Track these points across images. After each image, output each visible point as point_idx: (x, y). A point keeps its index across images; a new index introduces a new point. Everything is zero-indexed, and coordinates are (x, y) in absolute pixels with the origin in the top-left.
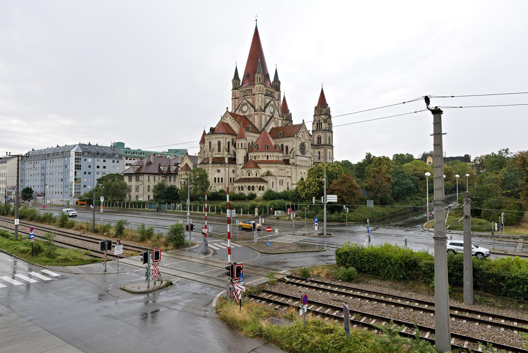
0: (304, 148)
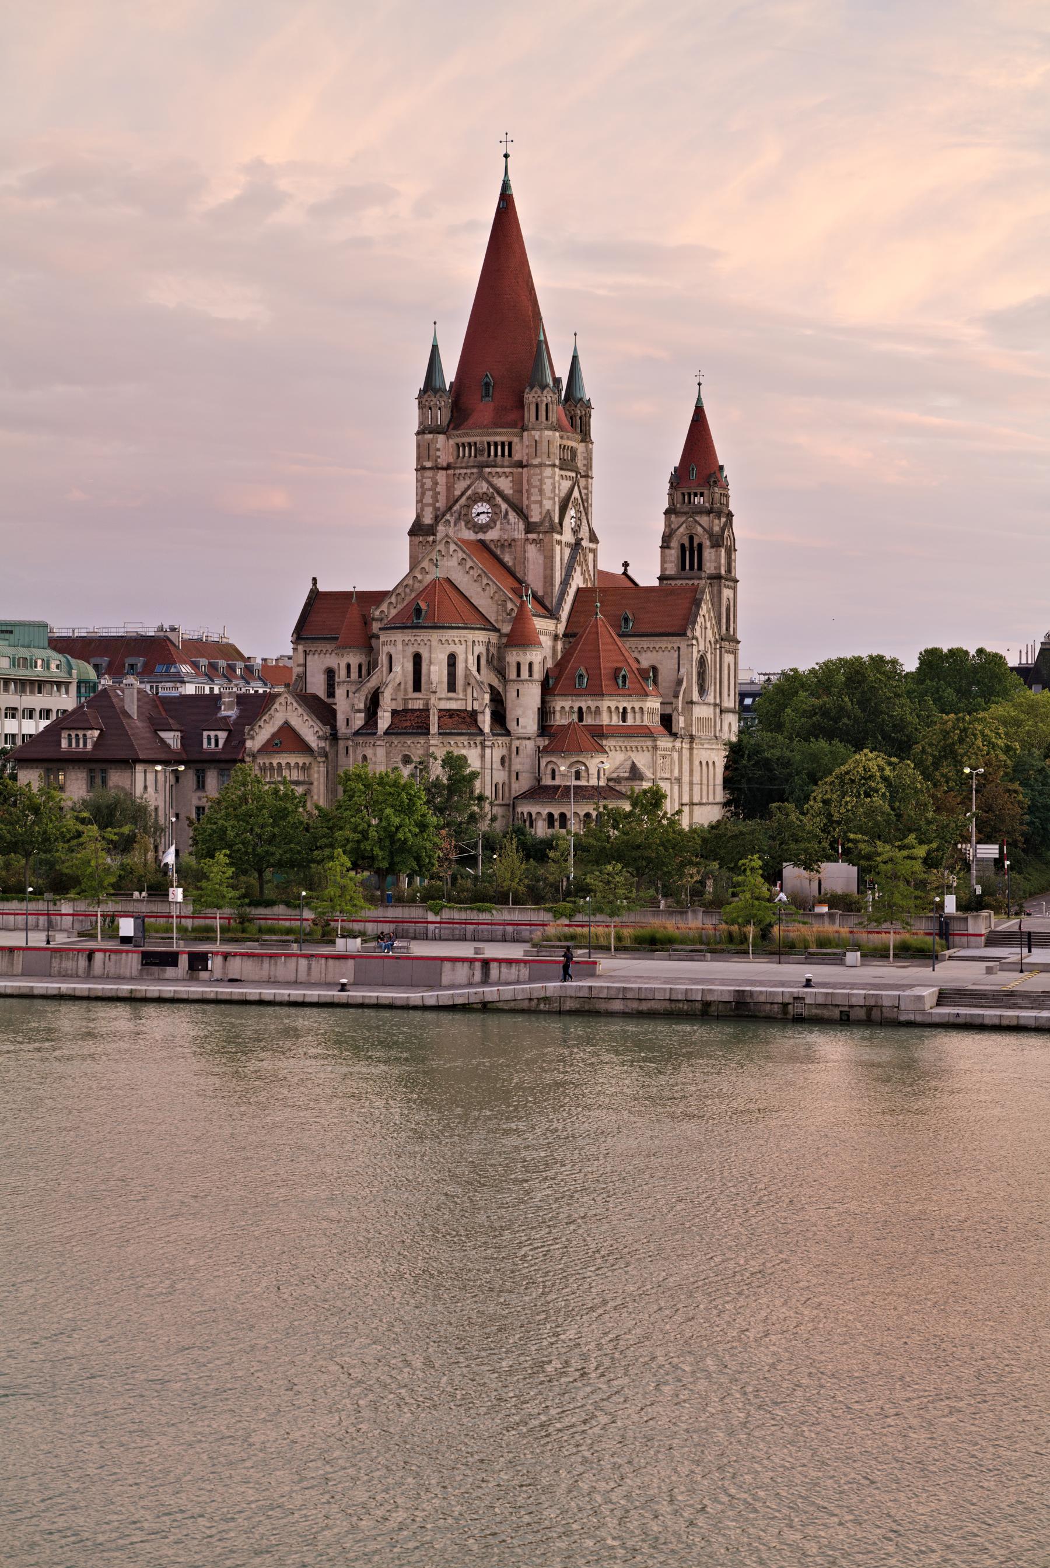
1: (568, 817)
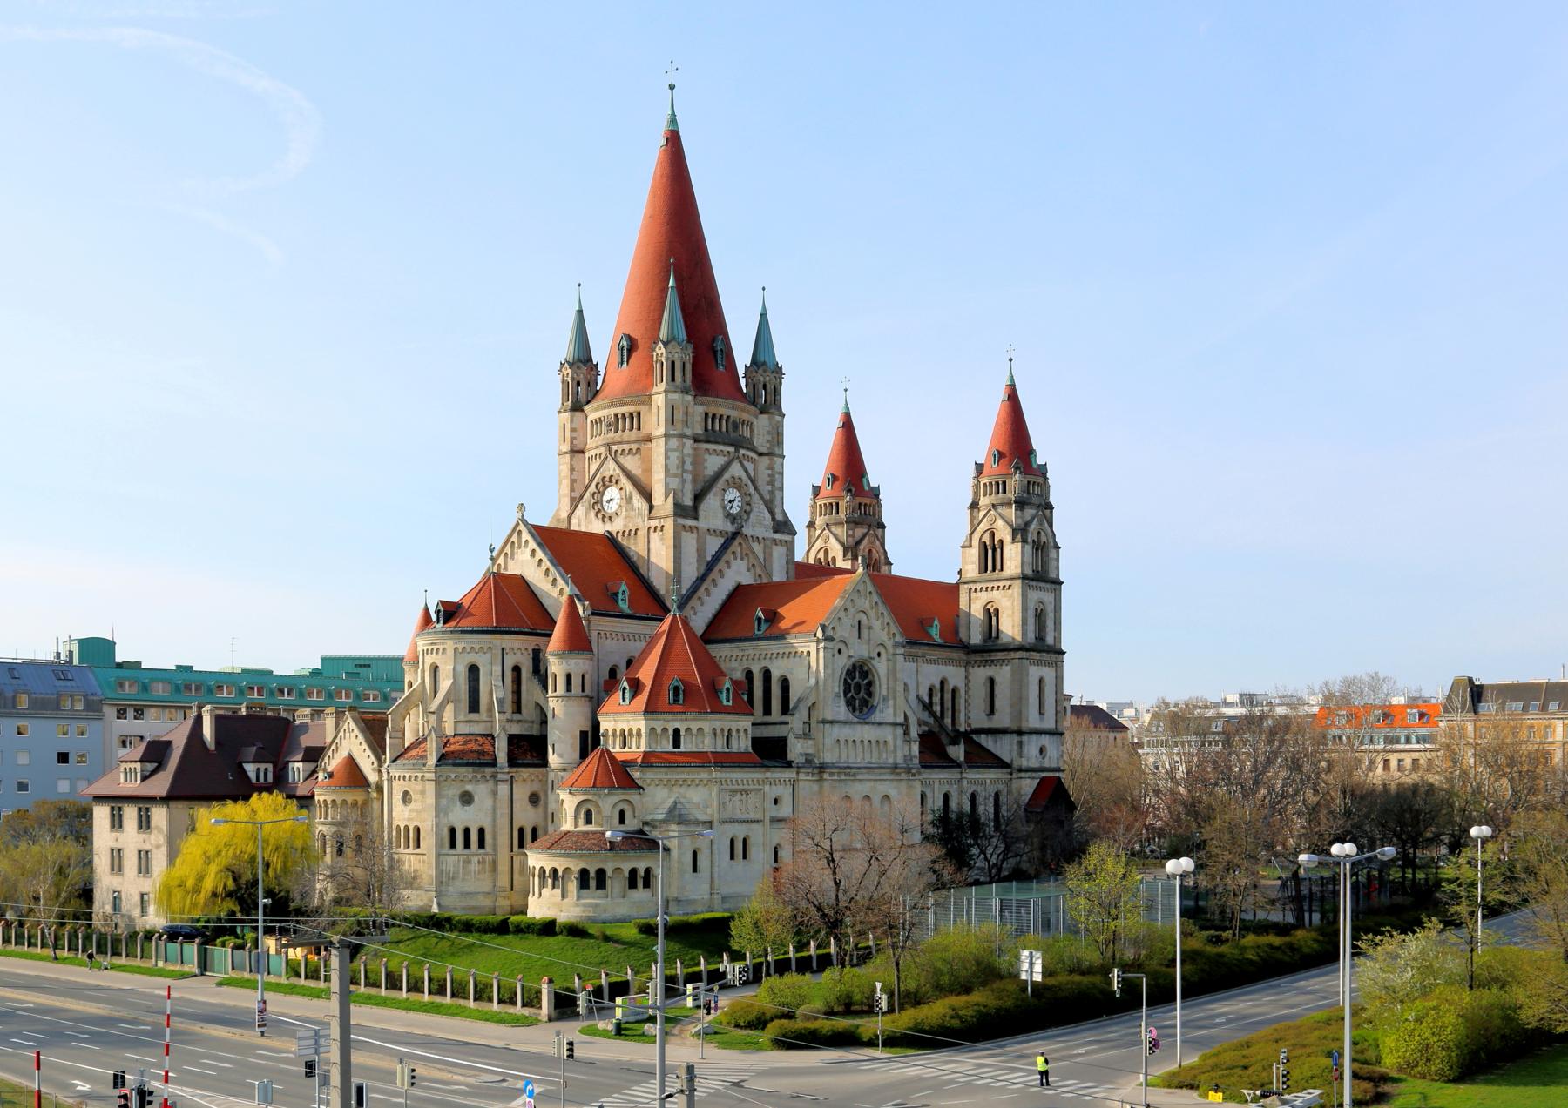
0: (870, 684)
1: (609, 873)
